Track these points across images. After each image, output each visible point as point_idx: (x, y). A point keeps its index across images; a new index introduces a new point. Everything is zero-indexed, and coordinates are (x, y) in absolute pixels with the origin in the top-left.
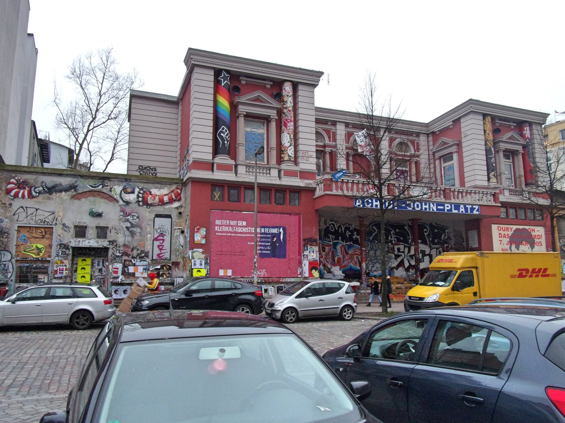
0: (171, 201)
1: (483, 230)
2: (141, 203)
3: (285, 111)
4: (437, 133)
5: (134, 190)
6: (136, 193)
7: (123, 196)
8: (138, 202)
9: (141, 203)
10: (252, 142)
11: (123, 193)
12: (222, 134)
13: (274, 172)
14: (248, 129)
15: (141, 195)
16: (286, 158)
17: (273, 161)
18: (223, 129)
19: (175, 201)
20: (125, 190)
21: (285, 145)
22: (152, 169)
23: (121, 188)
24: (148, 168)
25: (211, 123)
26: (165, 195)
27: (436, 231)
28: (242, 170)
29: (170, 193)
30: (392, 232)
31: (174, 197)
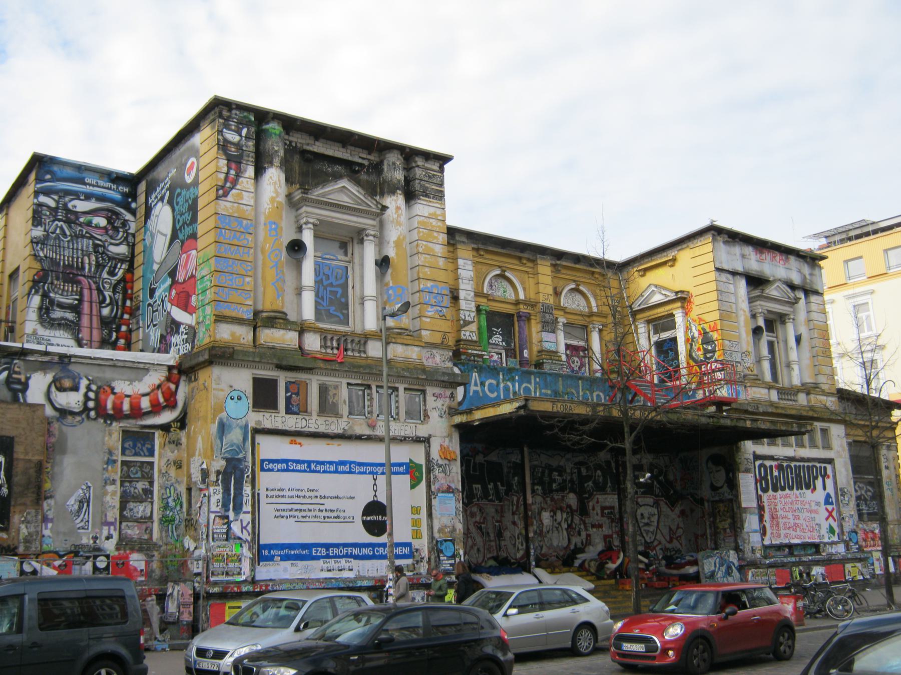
0: (156, 409)
2: (93, 414)
5: (79, 383)
6: (83, 389)
7: (53, 396)
8: (86, 409)
9: (93, 414)
10: (325, 283)
11: (53, 389)
15: (92, 395)
19: (164, 407)
20: (57, 385)
23: (49, 377)
26: (144, 395)
29: (153, 390)
31: (161, 400)
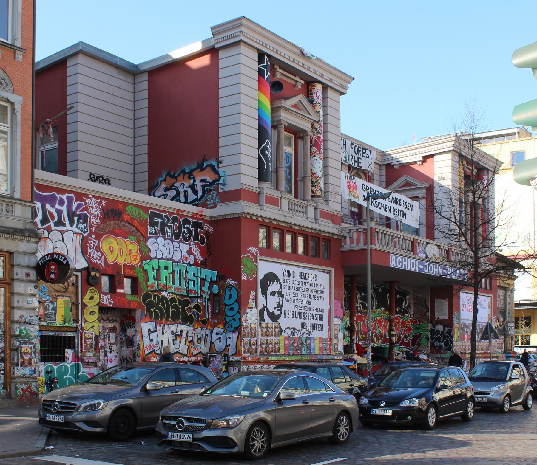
1: (454, 300)
3: (317, 126)
4: (396, 167)
12: (266, 152)
13: (311, 210)
14: (285, 148)
16: (318, 193)
17: (309, 195)
18: (267, 144)
21: (317, 174)
22: (105, 180)
24: (101, 179)
25: (256, 134)
27: (398, 296)
28: (285, 203)
30: (358, 296)
